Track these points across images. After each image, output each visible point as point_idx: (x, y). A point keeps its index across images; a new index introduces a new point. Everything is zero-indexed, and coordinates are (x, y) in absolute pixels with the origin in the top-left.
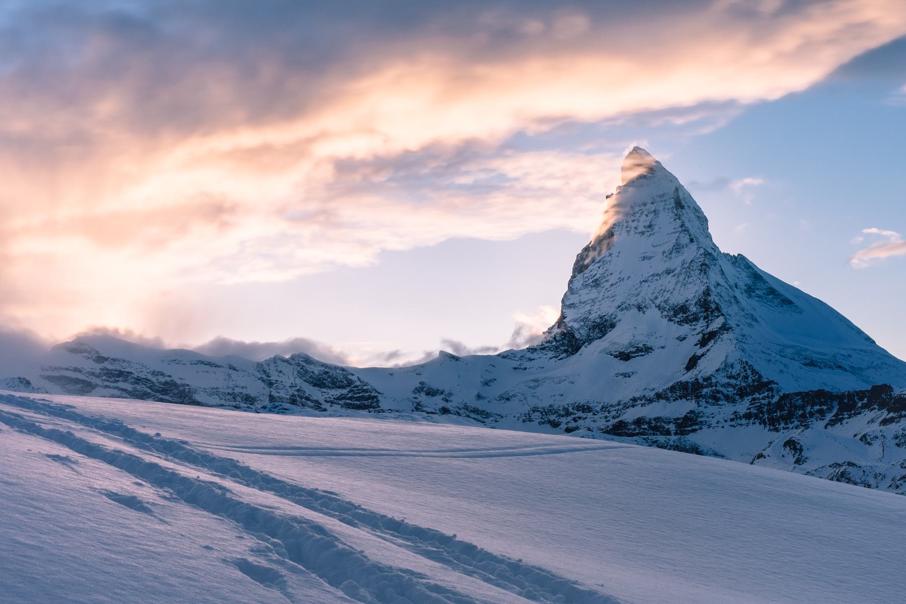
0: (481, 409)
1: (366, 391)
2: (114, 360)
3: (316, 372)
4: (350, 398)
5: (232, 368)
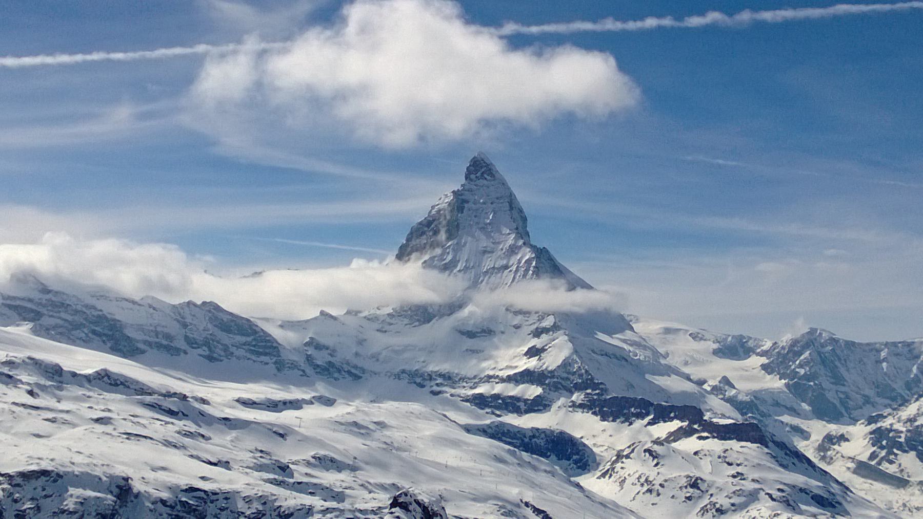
0: (360, 365)
1: (267, 341)
2: (57, 292)
3: (225, 320)
4: (254, 346)
5: (150, 306)
